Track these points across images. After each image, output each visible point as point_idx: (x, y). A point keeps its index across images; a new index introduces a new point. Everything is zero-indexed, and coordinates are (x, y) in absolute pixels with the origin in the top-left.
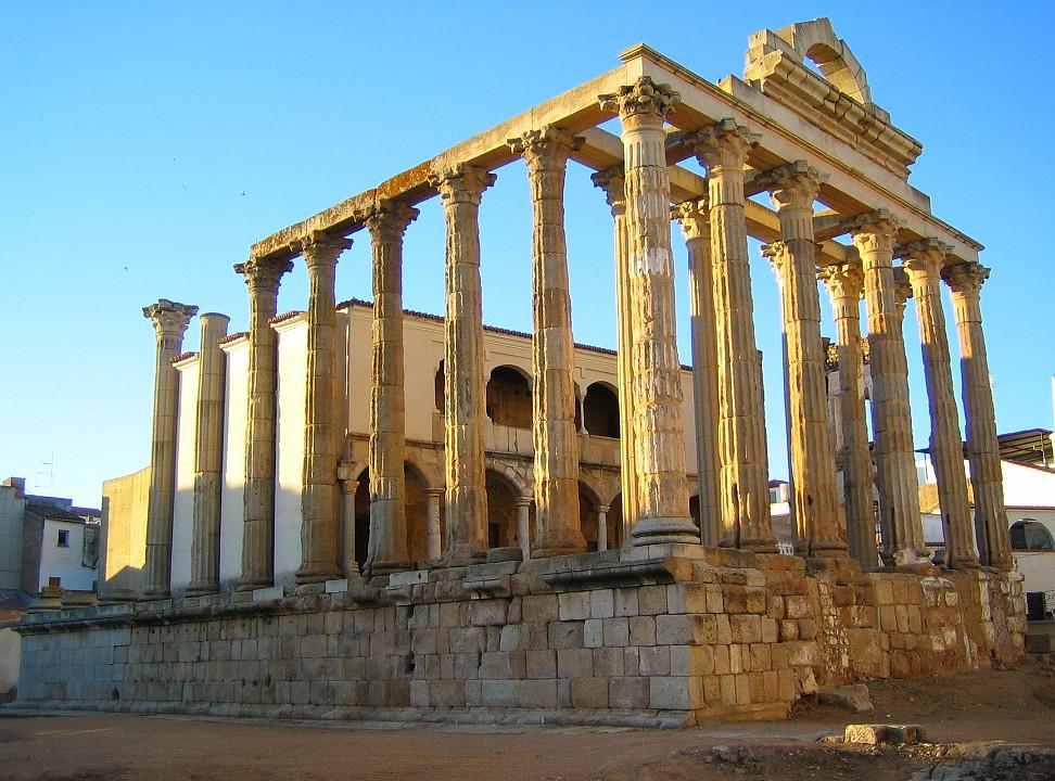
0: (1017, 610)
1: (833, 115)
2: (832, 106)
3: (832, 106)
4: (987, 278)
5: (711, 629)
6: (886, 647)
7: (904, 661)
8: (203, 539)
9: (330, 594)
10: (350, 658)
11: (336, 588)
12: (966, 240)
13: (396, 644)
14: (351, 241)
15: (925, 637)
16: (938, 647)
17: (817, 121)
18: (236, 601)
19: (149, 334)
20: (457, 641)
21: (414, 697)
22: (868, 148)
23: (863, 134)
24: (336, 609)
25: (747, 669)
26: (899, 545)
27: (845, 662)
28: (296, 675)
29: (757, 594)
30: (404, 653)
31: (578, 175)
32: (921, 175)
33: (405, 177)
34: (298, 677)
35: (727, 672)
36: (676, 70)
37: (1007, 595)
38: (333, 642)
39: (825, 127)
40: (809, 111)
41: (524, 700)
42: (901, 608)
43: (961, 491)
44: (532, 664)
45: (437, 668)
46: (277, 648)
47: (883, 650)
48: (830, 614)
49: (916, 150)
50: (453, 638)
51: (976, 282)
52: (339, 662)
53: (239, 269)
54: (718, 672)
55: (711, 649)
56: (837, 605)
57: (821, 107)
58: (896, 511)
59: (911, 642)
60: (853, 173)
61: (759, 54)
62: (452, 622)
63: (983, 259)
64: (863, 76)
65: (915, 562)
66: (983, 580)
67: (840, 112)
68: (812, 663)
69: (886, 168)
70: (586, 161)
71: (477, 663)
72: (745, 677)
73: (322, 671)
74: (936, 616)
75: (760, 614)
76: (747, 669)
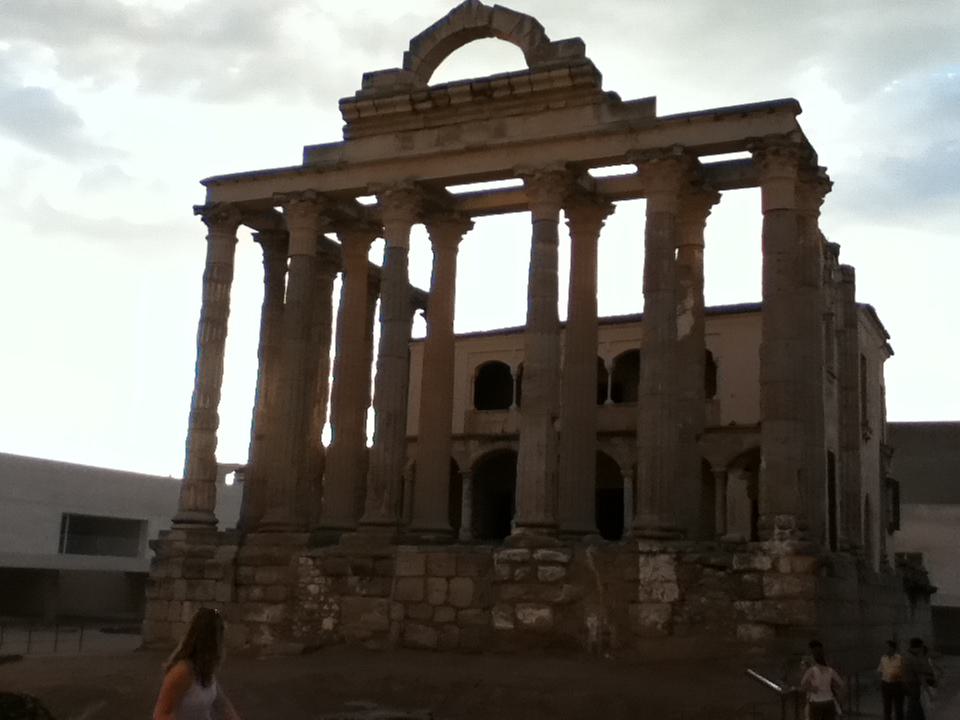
1: (436, 108)
3: (427, 105)
15: (470, 612)
16: (502, 624)
17: (421, 125)
22: (508, 108)
23: (491, 99)
27: (328, 623)
29: (215, 566)
56: (325, 573)
60: (482, 149)
69: (548, 108)
74: (511, 591)
75: (217, 580)
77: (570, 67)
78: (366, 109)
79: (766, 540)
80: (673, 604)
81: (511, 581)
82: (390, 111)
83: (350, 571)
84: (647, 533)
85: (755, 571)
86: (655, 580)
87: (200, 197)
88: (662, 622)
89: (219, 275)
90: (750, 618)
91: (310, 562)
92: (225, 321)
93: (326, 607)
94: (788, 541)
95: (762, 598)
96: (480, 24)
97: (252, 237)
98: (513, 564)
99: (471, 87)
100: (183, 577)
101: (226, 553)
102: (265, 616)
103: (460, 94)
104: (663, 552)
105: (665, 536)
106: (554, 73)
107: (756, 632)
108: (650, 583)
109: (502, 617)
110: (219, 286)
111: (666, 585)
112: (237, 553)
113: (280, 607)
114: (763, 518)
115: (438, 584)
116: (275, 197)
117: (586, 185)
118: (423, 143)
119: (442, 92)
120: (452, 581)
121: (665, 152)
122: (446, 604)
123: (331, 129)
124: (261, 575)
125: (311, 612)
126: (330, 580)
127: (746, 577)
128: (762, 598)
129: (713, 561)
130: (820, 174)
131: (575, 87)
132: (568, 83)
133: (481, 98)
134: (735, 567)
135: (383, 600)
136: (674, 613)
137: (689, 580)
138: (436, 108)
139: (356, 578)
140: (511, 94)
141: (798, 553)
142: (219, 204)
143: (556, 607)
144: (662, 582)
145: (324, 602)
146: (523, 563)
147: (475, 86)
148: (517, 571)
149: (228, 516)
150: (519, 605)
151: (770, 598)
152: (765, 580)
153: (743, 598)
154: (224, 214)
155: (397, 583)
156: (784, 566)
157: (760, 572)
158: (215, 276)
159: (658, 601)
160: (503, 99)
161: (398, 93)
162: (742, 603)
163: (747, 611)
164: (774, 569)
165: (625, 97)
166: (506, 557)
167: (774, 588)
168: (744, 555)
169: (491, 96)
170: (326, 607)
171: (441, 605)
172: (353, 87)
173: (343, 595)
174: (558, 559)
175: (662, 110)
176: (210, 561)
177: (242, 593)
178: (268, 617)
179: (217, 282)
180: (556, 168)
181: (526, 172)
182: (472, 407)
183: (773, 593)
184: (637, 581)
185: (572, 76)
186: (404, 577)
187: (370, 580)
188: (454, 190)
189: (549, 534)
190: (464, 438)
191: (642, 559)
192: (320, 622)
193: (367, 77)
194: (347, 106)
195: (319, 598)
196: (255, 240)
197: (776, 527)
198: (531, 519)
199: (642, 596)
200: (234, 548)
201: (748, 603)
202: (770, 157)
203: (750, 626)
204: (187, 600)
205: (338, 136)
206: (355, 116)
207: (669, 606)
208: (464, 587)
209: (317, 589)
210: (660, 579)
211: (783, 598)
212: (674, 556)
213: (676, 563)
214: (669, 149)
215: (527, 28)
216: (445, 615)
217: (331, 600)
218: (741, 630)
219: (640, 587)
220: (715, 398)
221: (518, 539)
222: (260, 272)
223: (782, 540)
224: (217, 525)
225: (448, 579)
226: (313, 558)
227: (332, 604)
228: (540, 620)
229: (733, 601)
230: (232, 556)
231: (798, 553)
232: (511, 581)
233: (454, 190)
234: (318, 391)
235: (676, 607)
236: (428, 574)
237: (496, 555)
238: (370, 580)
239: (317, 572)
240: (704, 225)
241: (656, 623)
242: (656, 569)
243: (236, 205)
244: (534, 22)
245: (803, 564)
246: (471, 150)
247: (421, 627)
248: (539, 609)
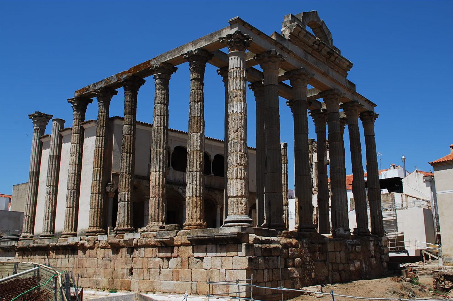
0: (385, 253)
3: (316, 46)
4: (377, 118)
5: (256, 263)
6: (330, 269)
7: (338, 274)
8: (48, 214)
9: (99, 241)
10: (106, 269)
11: (103, 239)
12: (369, 102)
13: (126, 264)
14: (117, 92)
16: (352, 268)
18: (61, 242)
19: (32, 127)
20: (151, 263)
21: (132, 287)
24: (102, 248)
25: (271, 280)
26: (338, 226)
27: (313, 275)
28: (83, 275)
30: (129, 267)
31: (211, 70)
32: (351, 76)
33: (138, 67)
34: (85, 276)
35: (262, 281)
36: (252, 28)
37: (381, 246)
38: (100, 262)
41: (177, 290)
42: (338, 253)
43: (364, 204)
44: (181, 275)
45: (142, 275)
46: (77, 263)
47: (329, 270)
48: (307, 256)
49: (350, 65)
50: (149, 262)
51: (373, 119)
52: (102, 270)
53: (69, 101)
54: (258, 281)
55: (256, 271)
58: (337, 212)
59: (341, 267)
61: (288, 25)
62: (150, 255)
63: (376, 110)
64: (330, 34)
65: (343, 233)
66: (372, 241)
70: (215, 64)
71: (159, 274)
72: (270, 283)
73: (95, 274)
74: (352, 256)
76: (271, 280)
118: (311, 60)
122: (341, 263)
125: (308, 270)
139: (318, 253)
150: (354, 261)
169: (330, 57)
192: (311, 275)
204: (265, 269)
225: (340, 251)
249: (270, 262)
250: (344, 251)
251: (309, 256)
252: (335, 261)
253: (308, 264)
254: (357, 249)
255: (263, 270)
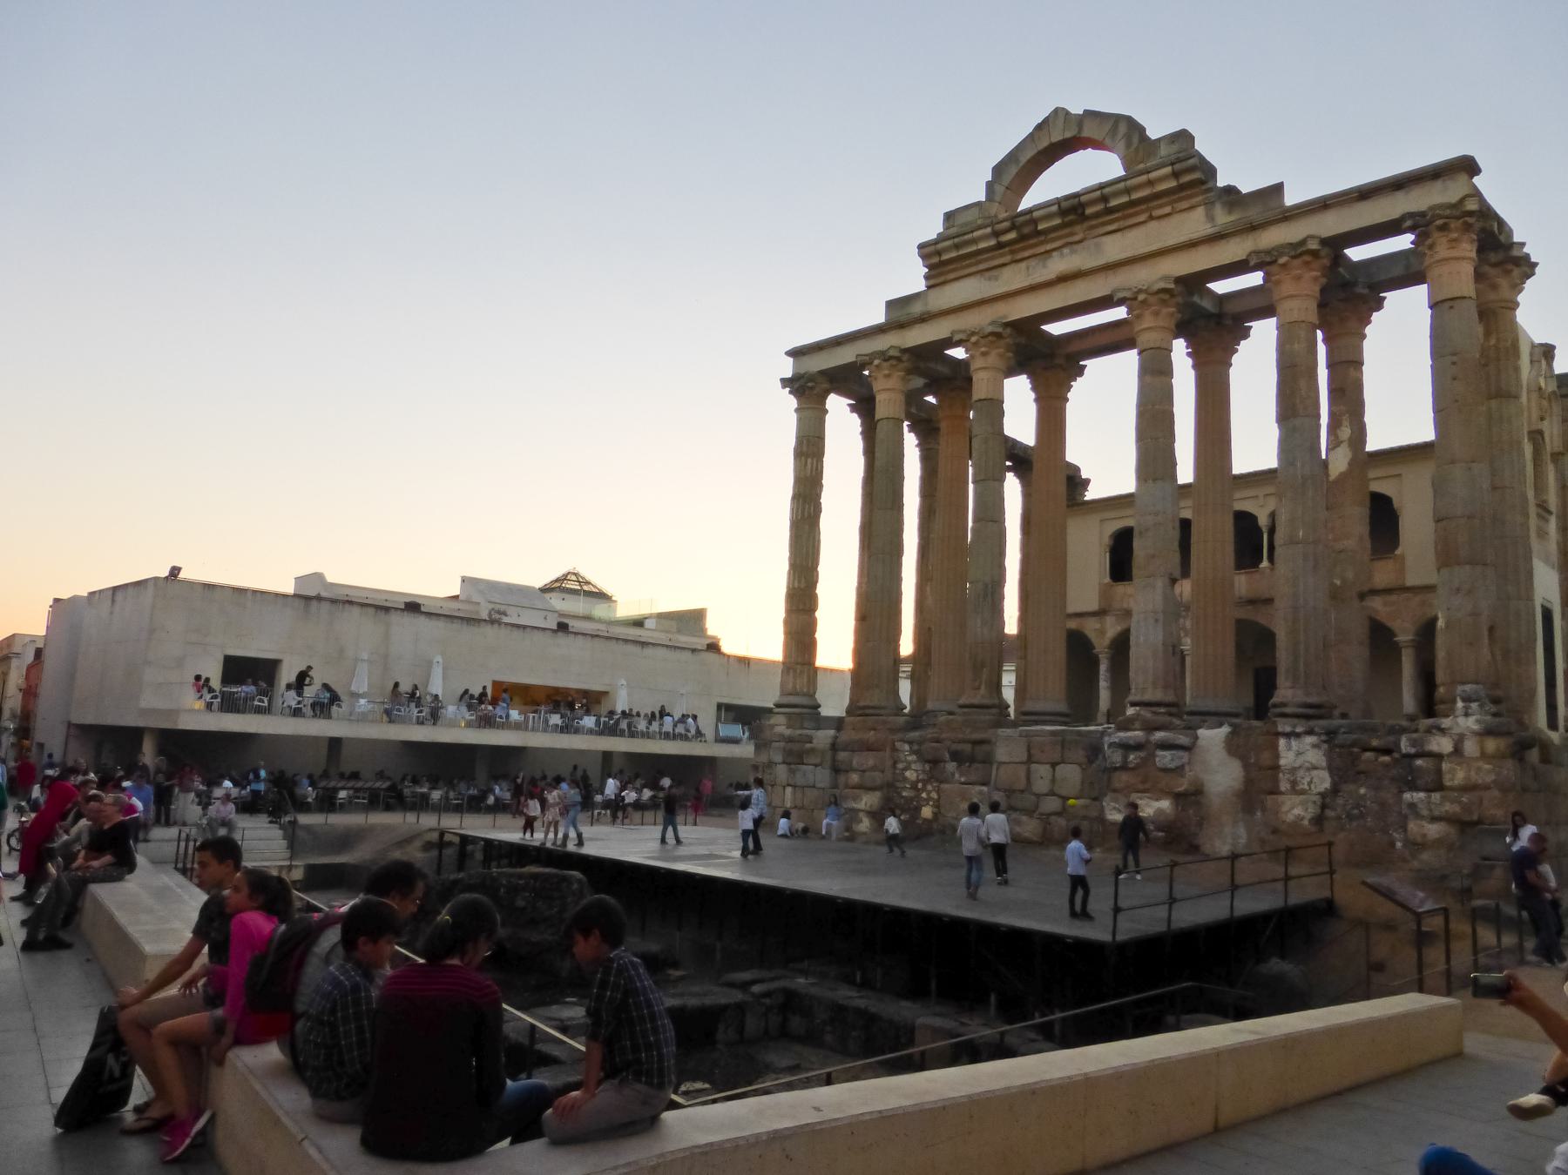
1: (1022, 238)
2: (1012, 235)
3: (1012, 235)
23: (1083, 218)
27: (927, 812)
29: (813, 750)
39: (1019, 256)
40: (992, 258)
54: (773, 804)
57: (1000, 246)
67: (1026, 230)
68: (868, 808)
74: (1122, 779)
75: (816, 765)
77: (1172, 164)
78: (946, 250)
79: (1448, 716)
80: (1323, 795)
81: (1124, 767)
82: (973, 248)
83: (947, 756)
84: (1288, 710)
85: (1430, 755)
86: (1300, 767)
87: (787, 368)
88: (1309, 816)
89: (810, 449)
90: (1425, 812)
91: (907, 747)
92: (819, 496)
93: (924, 795)
94: (1474, 717)
95: (1439, 787)
96: (1068, 135)
97: (848, 409)
98: (1126, 747)
99: (1059, 206)
100: (784, 763)
101: (823, 737)
102: (863, 802)
103: (1049, 217)
104: (1310, 732)
105: (1312, 713)
106: (1153, 175)
107: (1434, 830)
108: (1294, 770)
109: (1115, 808)
110: (809, 461)
111: (1315, 773)
112: (836, 737)
113: (878, 794)
114: (1441, 690)
115: (1042, 770)
116: (859, 359)
117: (1206, 304)
118: (1014, 277)
119: (1028, 217)
120: (1058, 768)
121: (1297, 250)
122: (1052, 793)
123: (912, 278)
124: (856, 760)
125: (909, 800)
126: (927, 767)
127: (1419, 762)
128: (1439, 787)
129: (1375, 743)
130: (1515, 253)
131: (1181, 188)
132: (1173, 184)
133: (1071, 217)
134: (1404, 751)
135: (985, 789)
136: (1324, 807)
137: (1344, 768)
138: (1022, 238)
140: (1106, 208)
141: (1488, 732)
142: (805, 374)
143: (1178, 797)
144: (1308, 769)
145: (924, 789)
146: (1138, 747)
147: (1065, 205)
148: (1132, 757)
149: (834, 703)
151: (1452, 789)
152: (1445, 766)
153: (1414, 787)
154: (810, 384)
155: (997, 769)
156: (1470, 747)
157: (1439, 757)
158: (805, 449)
159: (1303, 792)
160: (1097, 215)
161: (980, 228)
162: (1415, 794)
163: (1420, 806)
164: (1458, 751)
165: (1245, 188)
166: (1117, 740)
167: (1456, 775)
168: (1415, 735)
169: (1083, 213)
170: (924, 795)
171: (1047, 795)
172: (933, 228)
173: (941, 782)
174: (1178, 742)
175: (1291, 199)
176: (808, 745)
177: (842, 779)
178: (866, 804)
179: (807, 456)
180: (1162, 285)
181: (1127, 294)
182: (1107, 580)
183: (1456, 782)
184: (1276, 768)
185: (1176, 175)
186: (1004, 763)
187: (969, 766)
188: (1056, 329)
189: (1171, 714)
190: (1101, 613)
191: (1282, 742)
192: (918, 809)
193: (949, 217)
194: (927, 250)
195: (917, 786)
196: (852, 411)
197: (1458, 699)
198: (1148, 696)
199: (1284, 786)
200: (832, 732)
201: (1422, 795)
202: (1436, 235)
203: (1424, 823)
204: (789, 785)
205: (920, 285)
206: (935, 260)
207: (1317, 798)
208: (1071, 774)
209: (915, 775)
210: (1307, 764)
211: (1468, 788)
212: (1323, 738)
213: (1325, 746)
214: (1303, 242)
215: (1122, 129)
216: (1052, 804)
217: (929, 787)
218: (1412, 826)
219: (1281, 775)
220: (1398, 552)
221: (1132, 720)
222: (858, 444)
223: (1467, 715)
224: (819, 709)
225: (1054, 765)
226: (910, 743)
227: (931, 792)
228: (1160, 811)
229: (1401, 792)
230: (829, 741)
231: (1488, 732)
232: (1124, 767)
233: (1056, 329)
234: (930, 568)
235: (1326, 800)
236: (1030, 760)
237: (1106, 739)
238: (969, 766)
239: (914, 757)
240: (1364, 337)
241: (1302, 819)
242: (1299, 754)
243: (822, 373)
244: (1130, 121)
245: (1491, 745)
246: (1063, 279)
247: (1024, 818)
248: (1157, 800)
249: (798, 775)
250: (1080, 765)
251: (917, 771)
252: (1022, 784)
253: (908, 786)
254: (1157, 759)
255: (784, 787)
